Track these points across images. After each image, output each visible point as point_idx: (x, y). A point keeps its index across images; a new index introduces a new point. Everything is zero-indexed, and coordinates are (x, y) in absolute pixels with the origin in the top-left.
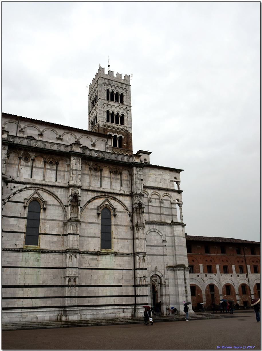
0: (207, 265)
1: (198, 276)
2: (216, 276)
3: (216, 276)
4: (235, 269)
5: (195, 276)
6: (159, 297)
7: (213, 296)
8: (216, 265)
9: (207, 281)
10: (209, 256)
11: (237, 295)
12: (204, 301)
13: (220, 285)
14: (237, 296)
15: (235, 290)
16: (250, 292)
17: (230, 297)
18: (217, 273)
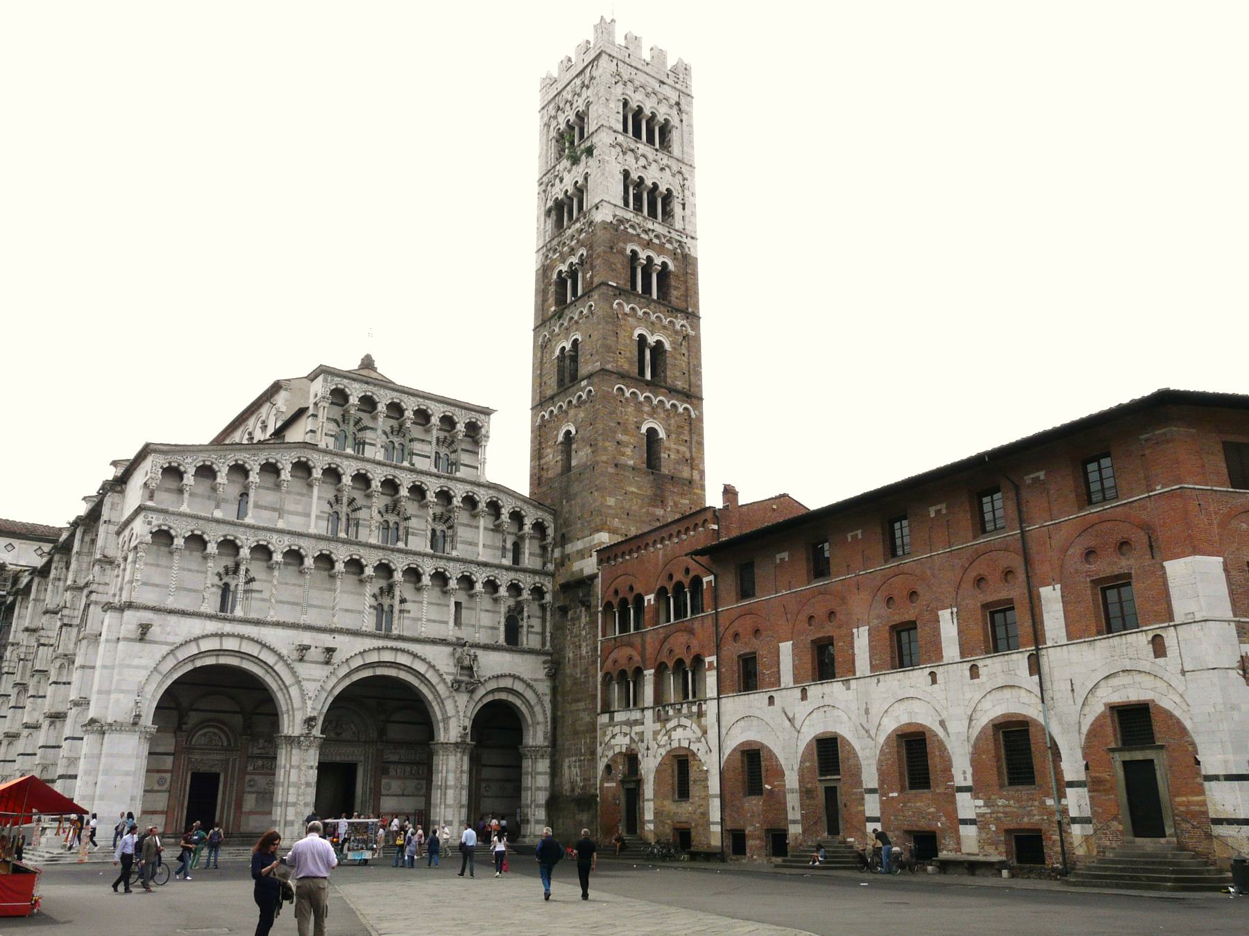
0: (813, 642)
1: (771, 699)
2: (848, 689)
3: (848, 689)
4: (960, 632)
5: (757, 700)
6: (648, 800)
7: (831, 793)
8: (855, 630)
9: (807, 722)
10: (822, 592)
11: (961, 789)
12: (794, 822)
13: (870, 736)
14: (963, 800)
15: (950, 760)
16: (1058, 773)
17: (918, 804)
18: (858, 675)
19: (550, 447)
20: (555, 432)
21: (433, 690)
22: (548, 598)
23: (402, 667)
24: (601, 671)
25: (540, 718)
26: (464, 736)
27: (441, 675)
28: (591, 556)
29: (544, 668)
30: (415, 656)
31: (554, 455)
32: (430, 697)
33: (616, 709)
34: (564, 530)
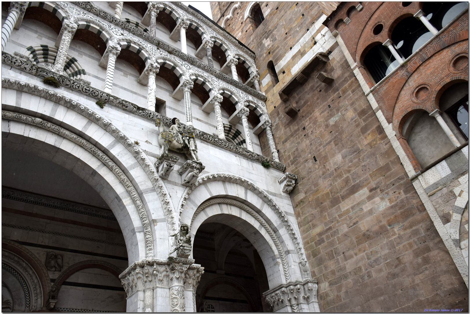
19: (237, 30)
20: (241, 17)
21: (123, 177)
22: (264, 118)
23: (67, 133)
24: (389, 122)
25: (289, 245)
26: (180, 251)
27: (136, 154)
28: (315, 43)
29: (281, 183)
30: (92, 119)
31: (242, 32)
32: (119, 189)
33: (458, 145)
34: (271, 59)
